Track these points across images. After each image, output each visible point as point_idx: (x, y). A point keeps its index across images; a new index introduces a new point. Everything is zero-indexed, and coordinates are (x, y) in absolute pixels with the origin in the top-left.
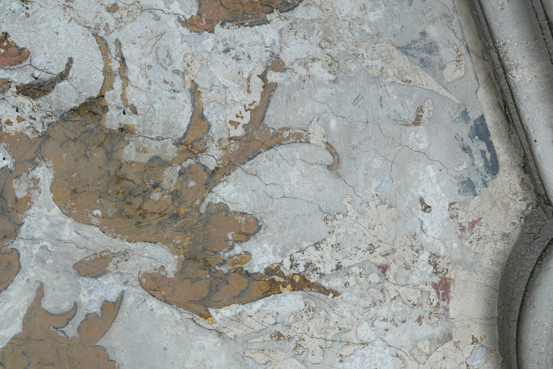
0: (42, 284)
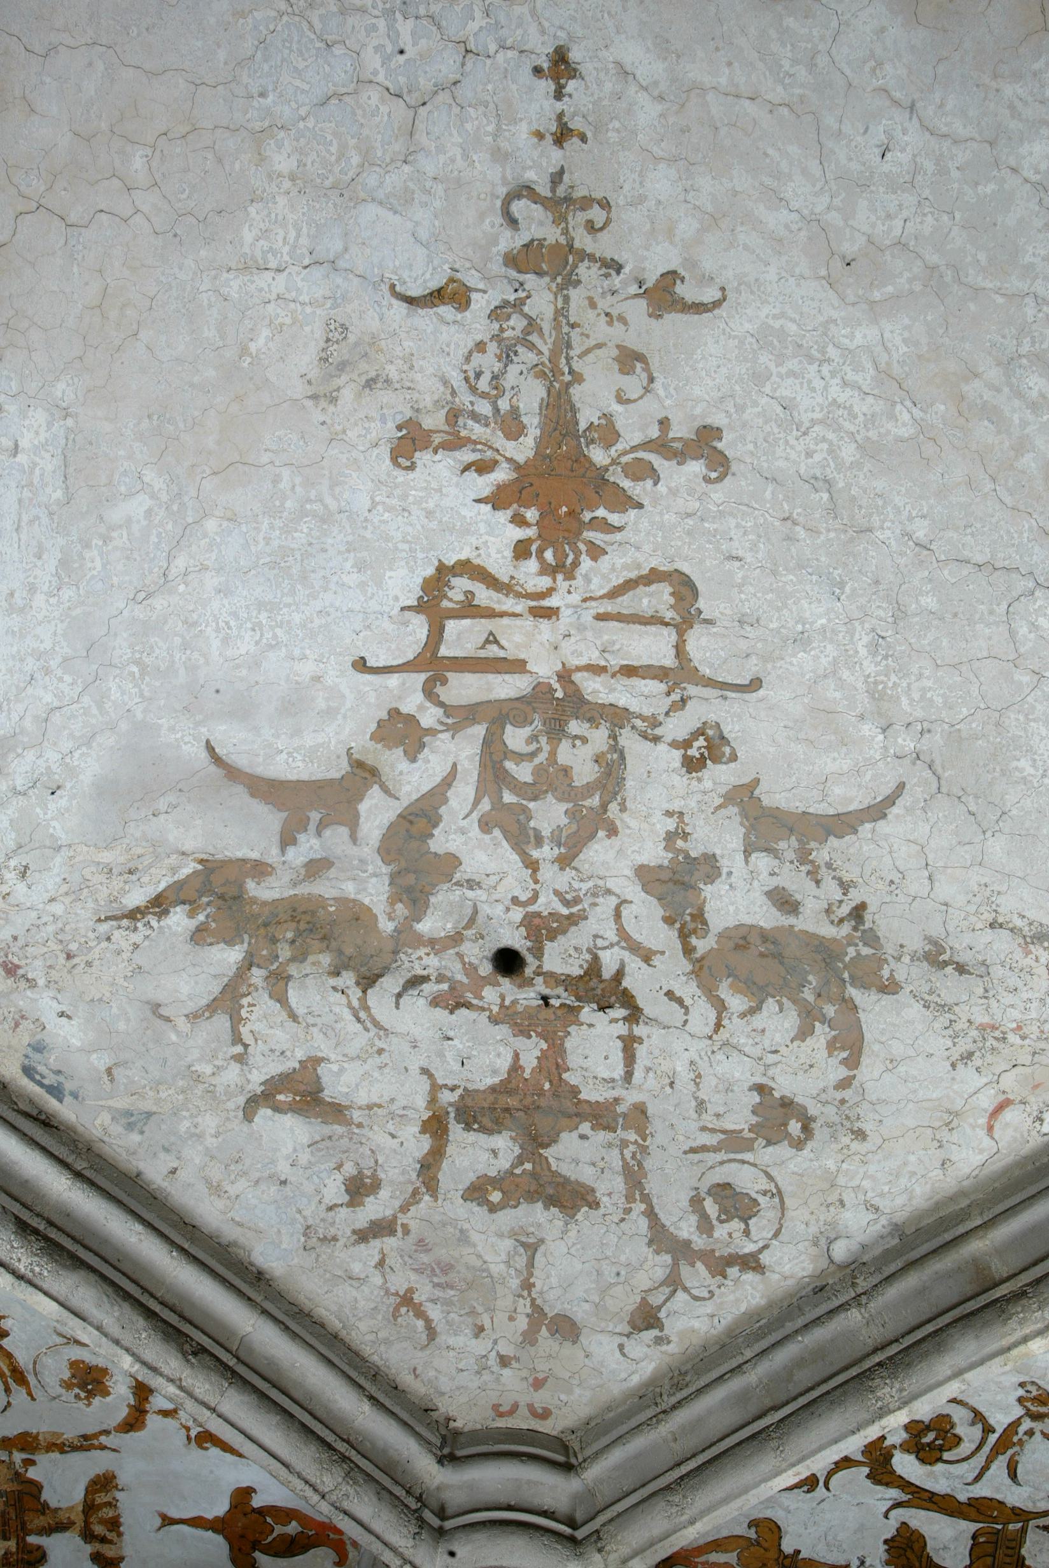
0: (355, 843)
